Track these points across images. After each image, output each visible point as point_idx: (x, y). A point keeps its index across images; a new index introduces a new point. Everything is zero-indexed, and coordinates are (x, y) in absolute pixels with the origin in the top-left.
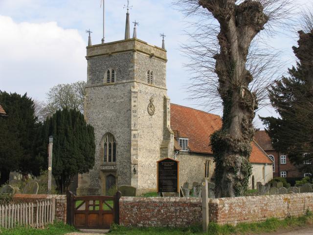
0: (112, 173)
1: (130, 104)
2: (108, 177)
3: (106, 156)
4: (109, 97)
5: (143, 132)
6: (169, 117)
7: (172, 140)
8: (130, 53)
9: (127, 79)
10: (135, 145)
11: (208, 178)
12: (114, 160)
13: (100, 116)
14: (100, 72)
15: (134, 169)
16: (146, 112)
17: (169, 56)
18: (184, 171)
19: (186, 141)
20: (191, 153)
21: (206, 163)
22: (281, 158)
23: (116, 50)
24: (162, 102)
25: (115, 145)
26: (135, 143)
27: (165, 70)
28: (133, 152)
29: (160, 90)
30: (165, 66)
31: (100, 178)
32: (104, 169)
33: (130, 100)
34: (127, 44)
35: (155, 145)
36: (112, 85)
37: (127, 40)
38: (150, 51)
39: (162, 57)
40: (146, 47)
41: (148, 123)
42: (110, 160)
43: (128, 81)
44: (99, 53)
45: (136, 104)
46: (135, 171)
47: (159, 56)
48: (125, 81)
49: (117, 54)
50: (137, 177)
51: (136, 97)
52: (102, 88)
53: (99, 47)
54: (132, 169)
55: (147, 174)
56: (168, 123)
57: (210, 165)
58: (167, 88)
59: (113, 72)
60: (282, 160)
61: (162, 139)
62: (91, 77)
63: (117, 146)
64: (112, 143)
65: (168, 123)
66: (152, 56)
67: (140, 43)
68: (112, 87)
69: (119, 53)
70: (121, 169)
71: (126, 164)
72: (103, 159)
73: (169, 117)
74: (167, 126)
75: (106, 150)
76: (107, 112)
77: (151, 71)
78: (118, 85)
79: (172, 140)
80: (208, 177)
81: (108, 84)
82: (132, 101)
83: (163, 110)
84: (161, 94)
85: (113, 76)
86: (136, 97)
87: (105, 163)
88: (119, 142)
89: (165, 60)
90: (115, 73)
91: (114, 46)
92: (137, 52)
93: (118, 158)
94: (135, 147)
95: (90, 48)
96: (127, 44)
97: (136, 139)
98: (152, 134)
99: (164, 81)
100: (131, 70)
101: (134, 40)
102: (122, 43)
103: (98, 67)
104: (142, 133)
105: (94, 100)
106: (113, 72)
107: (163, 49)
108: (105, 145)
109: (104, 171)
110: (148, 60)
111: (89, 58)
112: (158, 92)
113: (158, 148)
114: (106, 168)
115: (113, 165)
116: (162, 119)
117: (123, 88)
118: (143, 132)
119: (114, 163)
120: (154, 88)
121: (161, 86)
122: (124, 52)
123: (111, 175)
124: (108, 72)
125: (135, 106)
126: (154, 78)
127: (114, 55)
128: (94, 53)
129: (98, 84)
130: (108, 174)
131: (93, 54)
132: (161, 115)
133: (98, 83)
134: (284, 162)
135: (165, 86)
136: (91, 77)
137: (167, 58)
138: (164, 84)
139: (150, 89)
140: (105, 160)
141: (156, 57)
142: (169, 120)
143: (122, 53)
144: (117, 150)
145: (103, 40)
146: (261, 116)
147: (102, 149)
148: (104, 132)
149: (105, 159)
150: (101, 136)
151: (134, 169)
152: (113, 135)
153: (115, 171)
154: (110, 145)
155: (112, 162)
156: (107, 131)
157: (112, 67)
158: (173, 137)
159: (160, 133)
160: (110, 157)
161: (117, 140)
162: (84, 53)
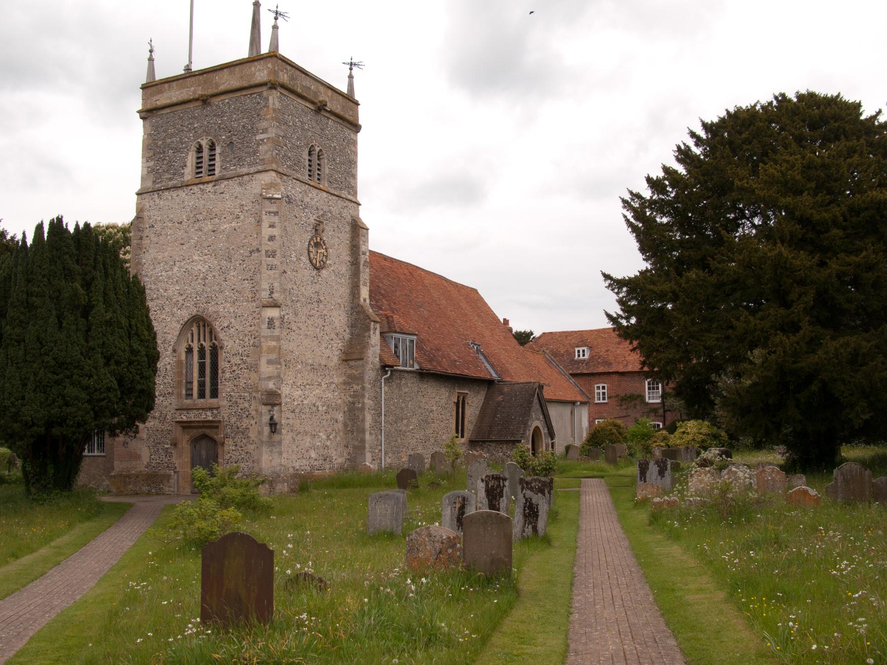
0: (208, 431)
1: (259, 233)
2: (195, 441)
3: (191, 383)
4: (200, 217)
5: (296, 315)
6: (365, 275)
7: (375, 338)
8: (260, 94)
9: (250, 165)
10: (270, 350)
11: (463, 440)
12: (215, 394)
13: (176, 269)
14: (177, 150)
15: (272, 418)
16: (304, 259)
17: (363, 117)
18: (405, 422)
19: (413, 341)
20: (424, 375)
21: (458, 401)
22: (596, 391)
23: (222, 88)
24: (345, 236)
25: (215, 352)
26: (274, 343)
27: (356, 154)
28: (266, 369)
29: (341, 203)
30: (355, 143)
31: (175, 444)
32: (185, 419)
33: (259, 222)
34: (258, 65)
35: (328, 352)
36: (208, 183)
37: (256, 58)
38: (316, 94)
39: (347, 116)
40: (307, 82)
41: (309, 291)
42: (202, 395)
43: (252, 170)
44: (174, 100)
45: (276, 232)
46: (273, 426)
47: (338, 110)
48: (245, 170)
49: (222, 97)
50: (280, 443)
51: (276, 213)
52: (182, 194)
53: (174, 84)
54: (266, 419)
55: (306, 433)
56: (365, 293)
57: (467, 407)
58: (360, 198)
59: (212, 148)
60: (599, 394)
61: (347, 336)
62: (151, 164)
63: (222, 356)
64: (207, 345)
65: (365, 293)
66: (320, 108)
67: (289, 68)
68: (209, 187)
69: (231, 95)
70: (233, 420)
71: (246, 405)
72: (184, 392)
73: (365, 275)
74: (362, 300)
75: (189, 366)
76: (196, 258)
77: (318, 149)
78: (226, 183)
79: (375, 338)
80: (462, 436)
81: (197, 181)
82: (265, 224)
83: (348, 258)
84: (345, 213)
85: (212, 158)
86: (276, 213)
87: (189, 401)
88: (226, 343)
89: (356, 128)
90: (218, 150)
91: (217, 77)
92: (279, 89)
93: (225, 388)
94: (273, 356)
95: (150, 87)
96: (253, 69)
97: (277, 332)
98: (320, 322)
99: (351, 180)
100: (262, 140)
101: (274, 55)
102: (237, 69)
103: (172, 135)
104: (291, 317)
105: (158, 227)
106: (212, 148)
107: (350, 100)
108: (190, 350)
109: (186, 426)
110: (309, 119)
111: (147, 114)
112: (336, 206)
113: (335, 360)
114: (192, 416)
115: (211, 409)
116: (345, 281)
117: (238, 189)
118: (296, 315)
119: (215, 400)
120: (325, 194)
121: (344, 194)
122: (244, 93)
123: (205, 436)
124: (200, 150)
125: (272, 238)
126: (326, 170)
127: (216, 101)
128: (163, 99)
129: (171, 184)
130: (195, 433)
131: (159, 103)
132: (345, 269)
133: (171, 180)
134: (604, 399)
135: (355, 194)
136: (151, 164)
137: (361, 122)
138: (353, 190)
139: (316, 198)
140: (189, 395)
141: (331, 112)
142: (365, 284)
143: (238, 94)
144: (222, 364)
145: (188, 69)
146: (618, 275)
147: (179, 362)
148: (185, 314)
149: (187, 390)
150: (179, 326)
151: (272, 418)
152: (210, 325)
153: (214, 425)
154: (202, 350)
155: (209, 401)
156: (194, 313)
157: (208, 134)
158: (378, 332)
159: (340, 319)
160: (202, 385)
161: (221, 335)
162: (137, 103)
